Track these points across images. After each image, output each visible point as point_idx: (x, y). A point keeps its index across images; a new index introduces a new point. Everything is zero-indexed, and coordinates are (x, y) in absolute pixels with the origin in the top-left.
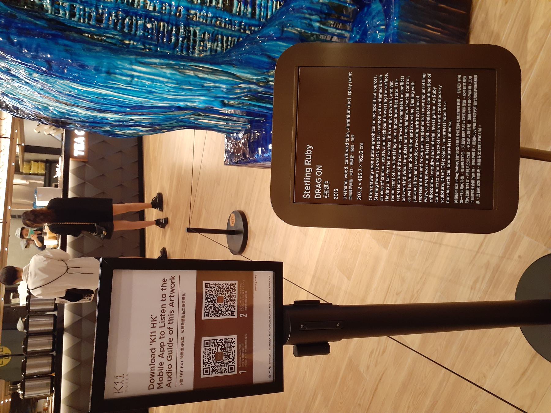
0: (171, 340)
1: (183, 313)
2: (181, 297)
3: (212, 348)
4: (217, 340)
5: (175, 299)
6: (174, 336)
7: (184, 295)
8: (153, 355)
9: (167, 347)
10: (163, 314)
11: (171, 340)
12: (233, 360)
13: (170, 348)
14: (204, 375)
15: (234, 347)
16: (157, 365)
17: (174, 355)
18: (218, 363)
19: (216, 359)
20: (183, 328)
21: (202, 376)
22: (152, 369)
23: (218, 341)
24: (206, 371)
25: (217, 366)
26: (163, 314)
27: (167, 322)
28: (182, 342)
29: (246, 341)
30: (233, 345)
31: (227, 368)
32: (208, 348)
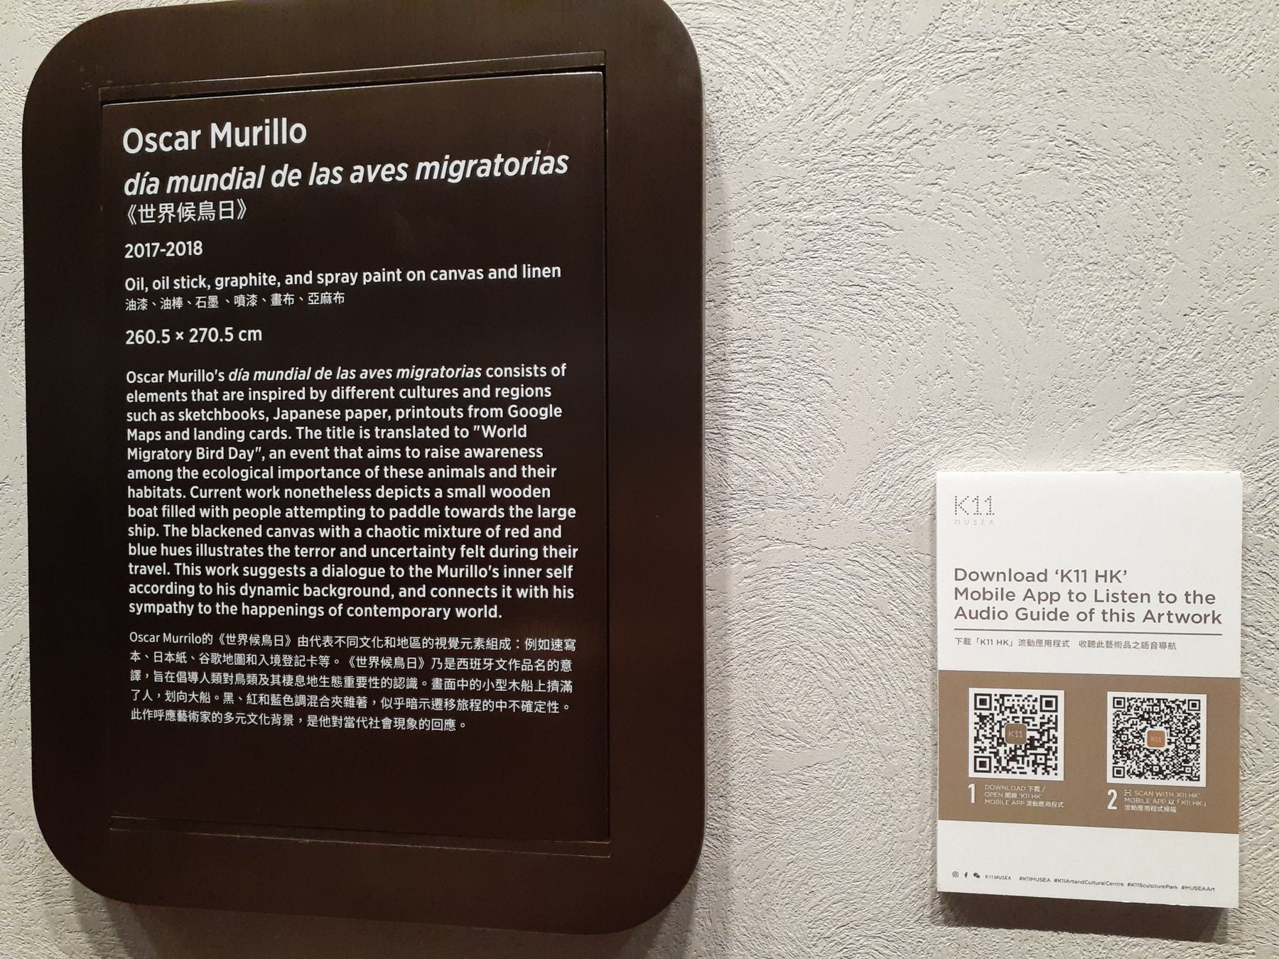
0: (1064, 616)
1: (1127, 645)
2: (1168, 639)
3: (1038, 717)
4: (1056, 729)
5: (1164, 625)
6: (1072, 623)
7: (1172, 646)
8: (1031, 577)
9: (1048, 607)
10: (1126, 598)
11: (1064, 616)
12: (1004, 769)
13: (1045, 616)
14: (976, 695)
15: (1035, 771)
16: (1009, 586)
17: (1028, 624)
18: (1000, 731)
19: (1009, 727)
20: (1091, 644)
21: (972, 691)
22: (1001, 576)
23: (1052, 732)
24: (983, 702)
25: (992, 729)
26: (1126, 598)
27: (1107, 606)
28: (1057, 643)
29: (1048, 804)
30: (1040, 770)
31: (986, 753)
32: (1037, 707)
